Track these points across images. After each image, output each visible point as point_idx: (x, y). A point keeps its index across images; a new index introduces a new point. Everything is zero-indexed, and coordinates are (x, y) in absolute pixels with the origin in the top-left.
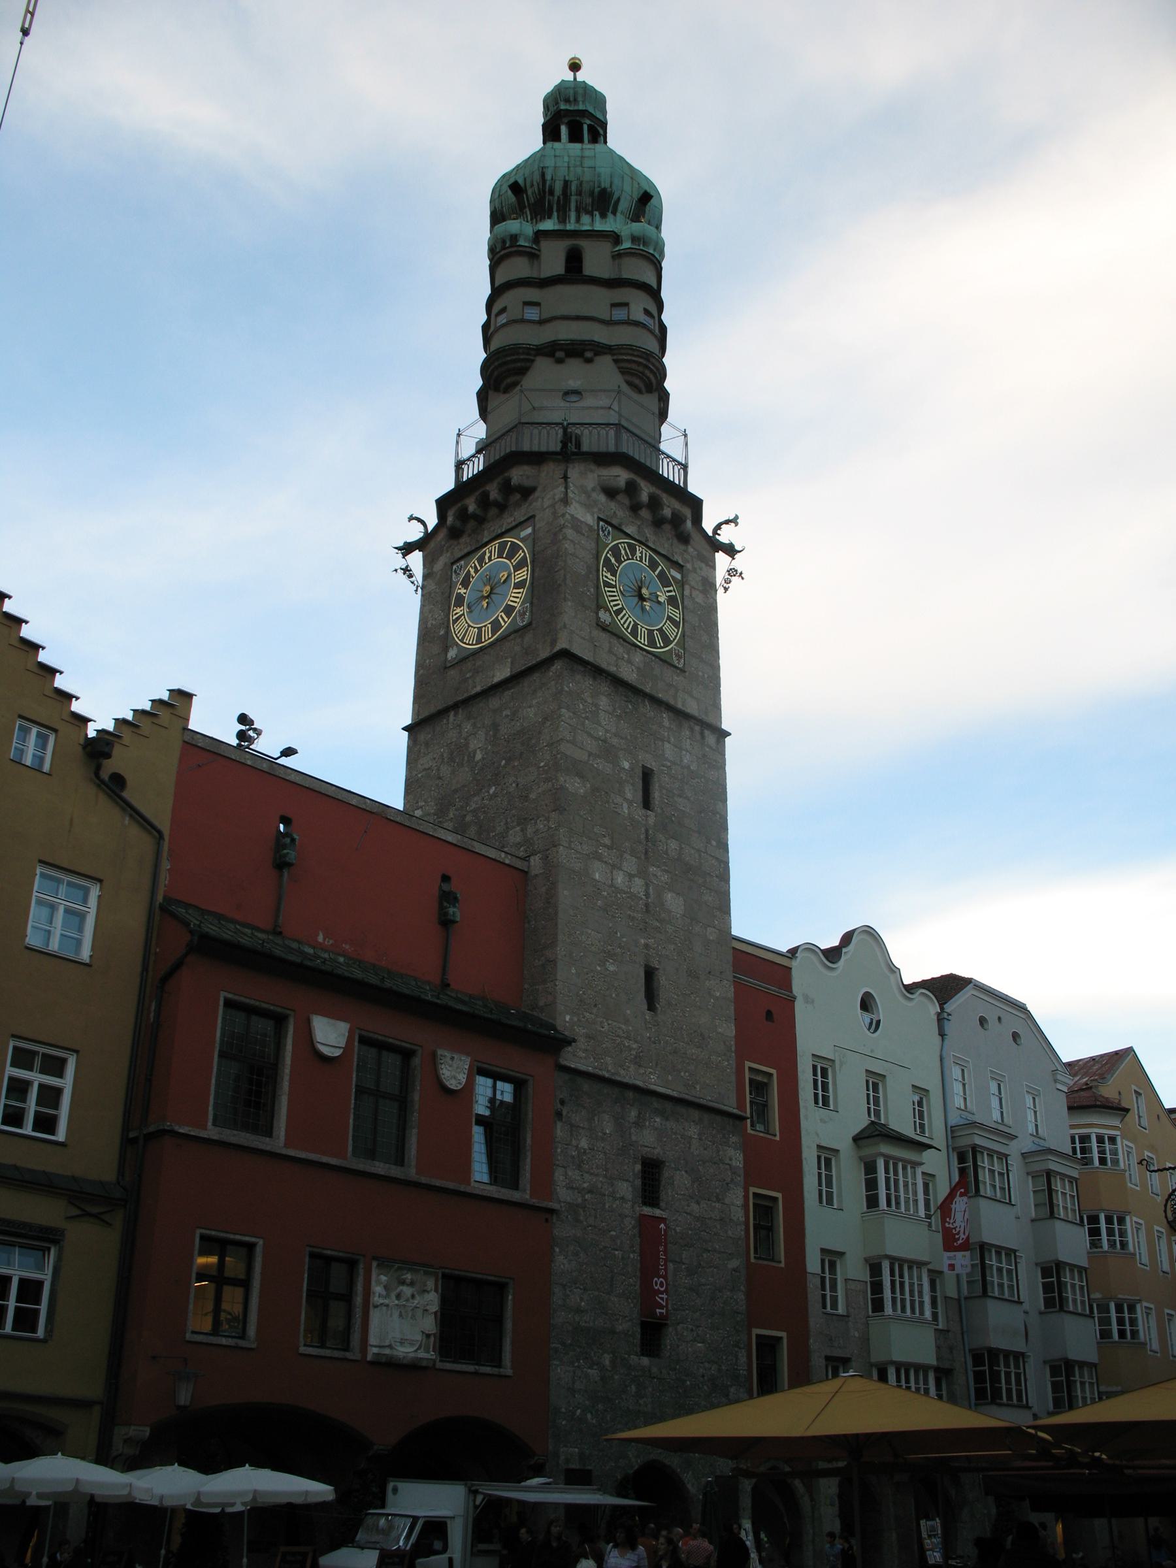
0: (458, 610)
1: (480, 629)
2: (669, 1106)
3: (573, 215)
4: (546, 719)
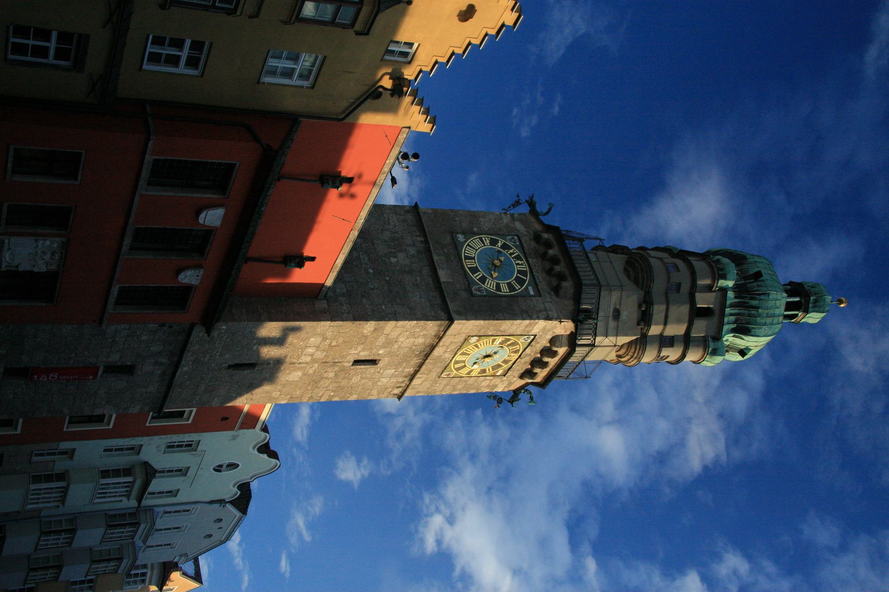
1: (473, 258)
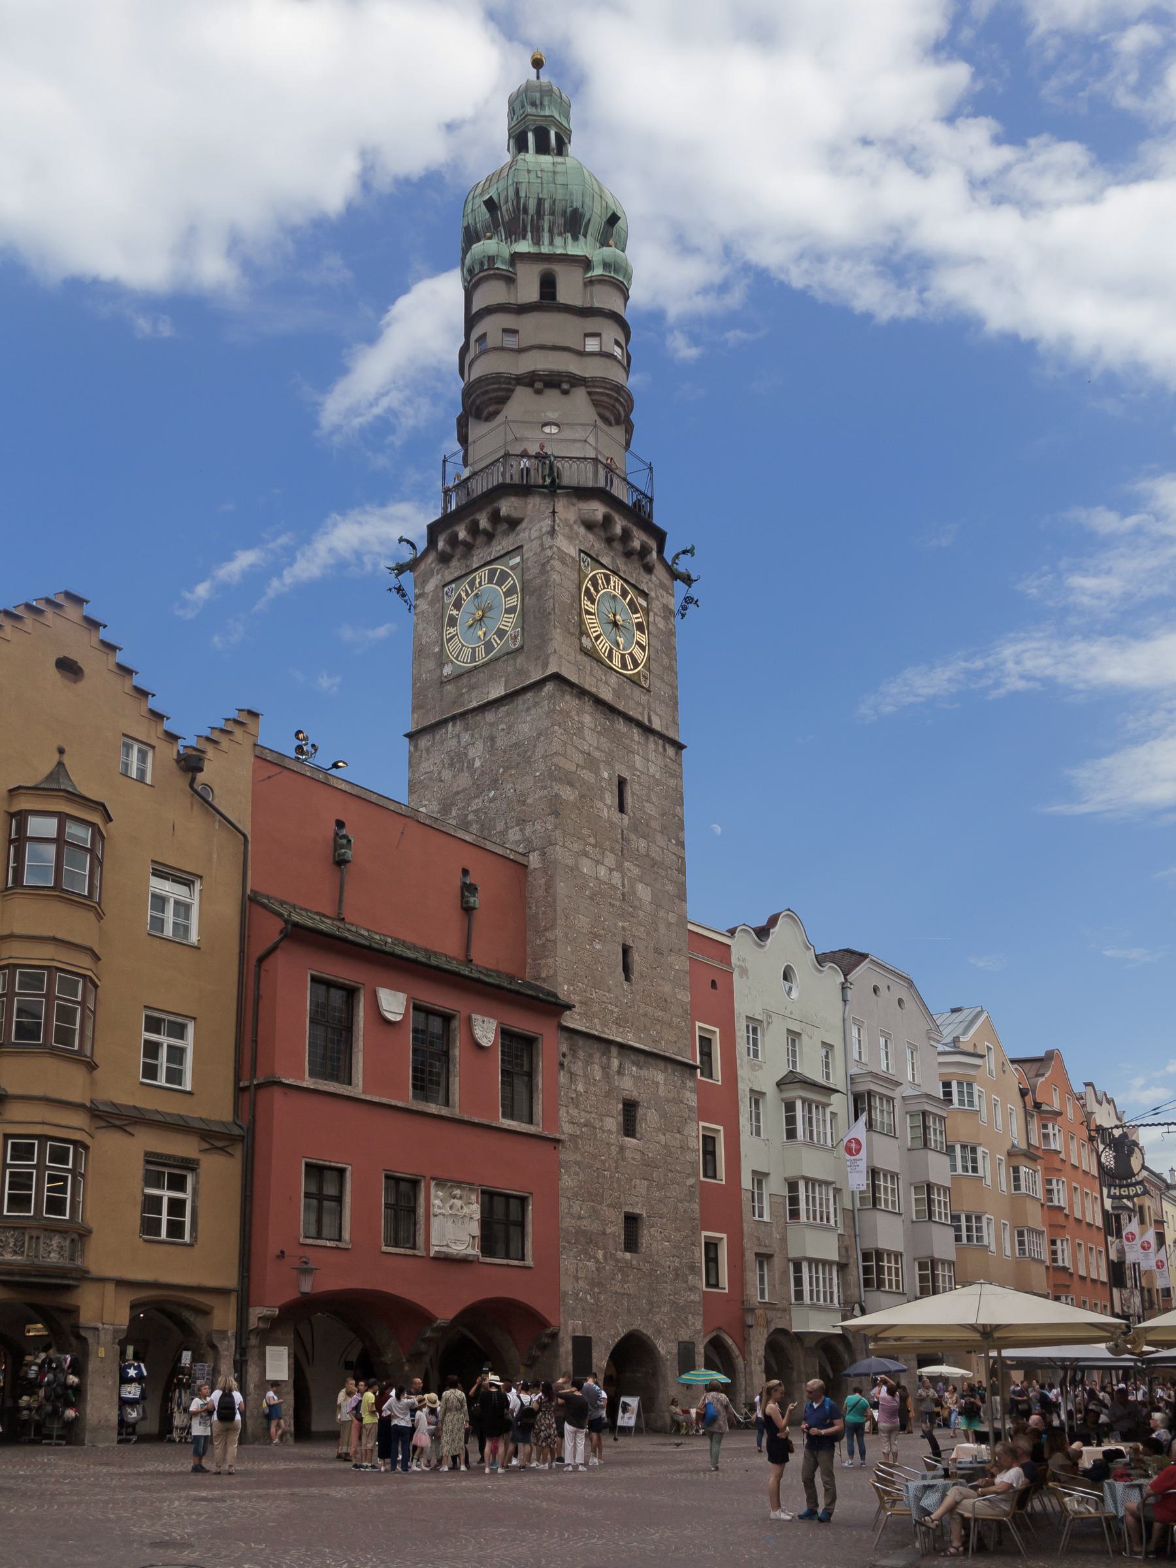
0: (452, 630)
1: (474, 649)
2: (642, 1058)
3: (546, 235)
4: (539, 735)
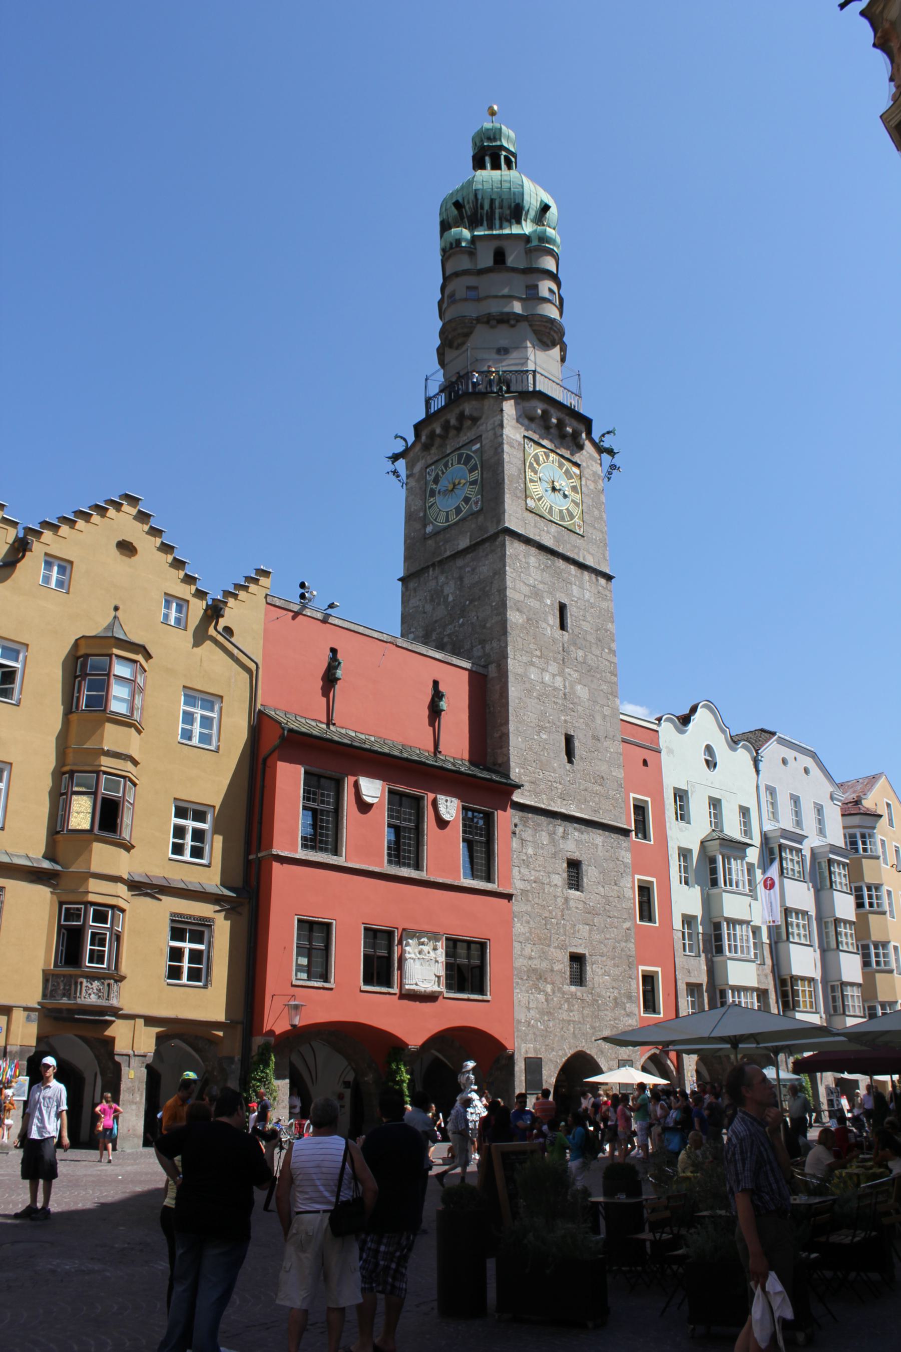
1: (447, 513)
3: (497, 222)
4: (495, 574)
